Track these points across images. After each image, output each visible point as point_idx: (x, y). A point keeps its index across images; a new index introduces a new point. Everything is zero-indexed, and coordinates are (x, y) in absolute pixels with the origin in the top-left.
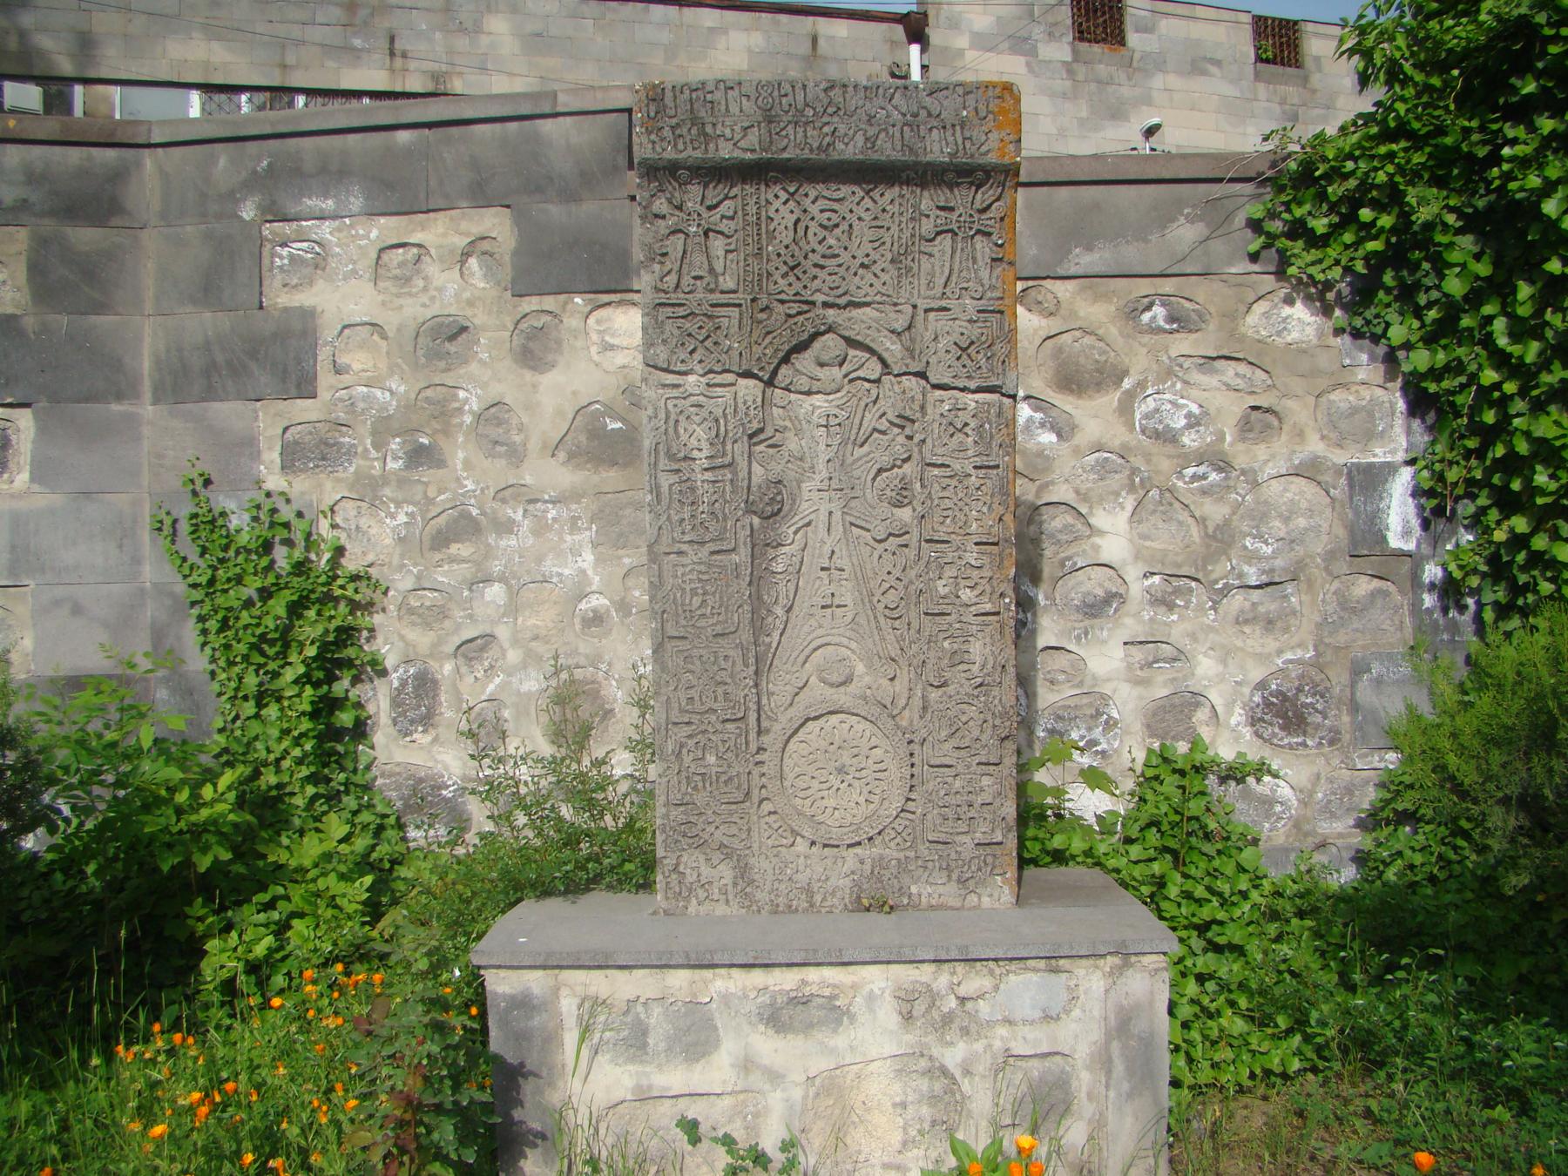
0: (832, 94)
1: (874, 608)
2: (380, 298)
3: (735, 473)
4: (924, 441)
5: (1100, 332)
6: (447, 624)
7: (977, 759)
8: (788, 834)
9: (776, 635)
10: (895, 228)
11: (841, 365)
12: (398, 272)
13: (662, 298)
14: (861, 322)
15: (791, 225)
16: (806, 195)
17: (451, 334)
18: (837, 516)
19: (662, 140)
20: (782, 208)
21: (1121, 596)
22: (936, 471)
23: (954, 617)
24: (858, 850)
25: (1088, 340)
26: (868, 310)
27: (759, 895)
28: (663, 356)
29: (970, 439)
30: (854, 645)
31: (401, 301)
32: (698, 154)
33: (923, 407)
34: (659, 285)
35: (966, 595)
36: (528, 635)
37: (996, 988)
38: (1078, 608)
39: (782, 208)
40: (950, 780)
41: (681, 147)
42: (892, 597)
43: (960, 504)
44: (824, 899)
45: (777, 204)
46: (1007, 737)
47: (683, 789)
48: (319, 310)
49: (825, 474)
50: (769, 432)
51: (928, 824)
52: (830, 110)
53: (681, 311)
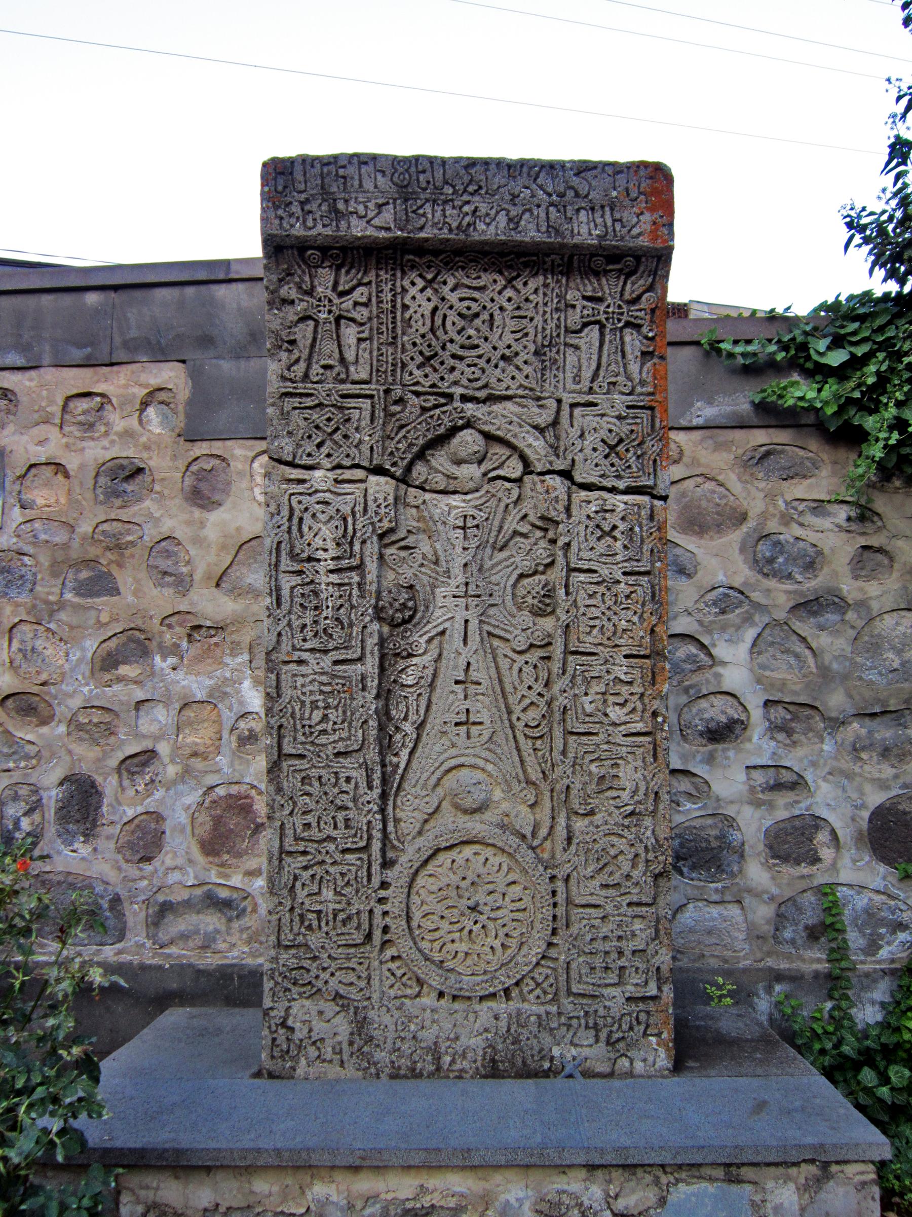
0: (473, 171)
1: (512, 727)
2: (64, 440)
3: (363, 576)
4: (568, 545)
5: (720, 478)
6: (112, 740)
7: (628, 899)
8: (413, 983)
9: (405, 754)
10: (538, 320)
11: (480, 462)
12: (81, 418)
13: (289, 387)
14: (499, 417)
15: (427, 313)
16: (445, 283)
17: (127, 475)
18: (474, 625)
19: (291, 215)
20: (418, 296)
21: (742, 722)
22: (582, 577)
23: (602, 736)
24: (492, 1004)
25: (710, 485)
26: (509, 405)
27: (379, 1055)
28: (289, 448)
29: (619, 544)
30: (490, 767)
31: (85, 444)
32: (328, 231)
33: (568, 509)
34: (286, 373)
35: (616, 713)
36: (188, 751)
37: (662, 1201)
38: (701, 734)
39: (418, 296)
40: (596, 922)
41: (310, 223)
42: (533, 715)
43: (608, 613)
44: (453, 1061)
45: (413, 291)
46: (660, 874)
47: (296, 929)
48: (8, 449)
49: (461, 579)
50: (402, 533)
51: (574, 974)
52: (471, 189)
53: (309, 402)
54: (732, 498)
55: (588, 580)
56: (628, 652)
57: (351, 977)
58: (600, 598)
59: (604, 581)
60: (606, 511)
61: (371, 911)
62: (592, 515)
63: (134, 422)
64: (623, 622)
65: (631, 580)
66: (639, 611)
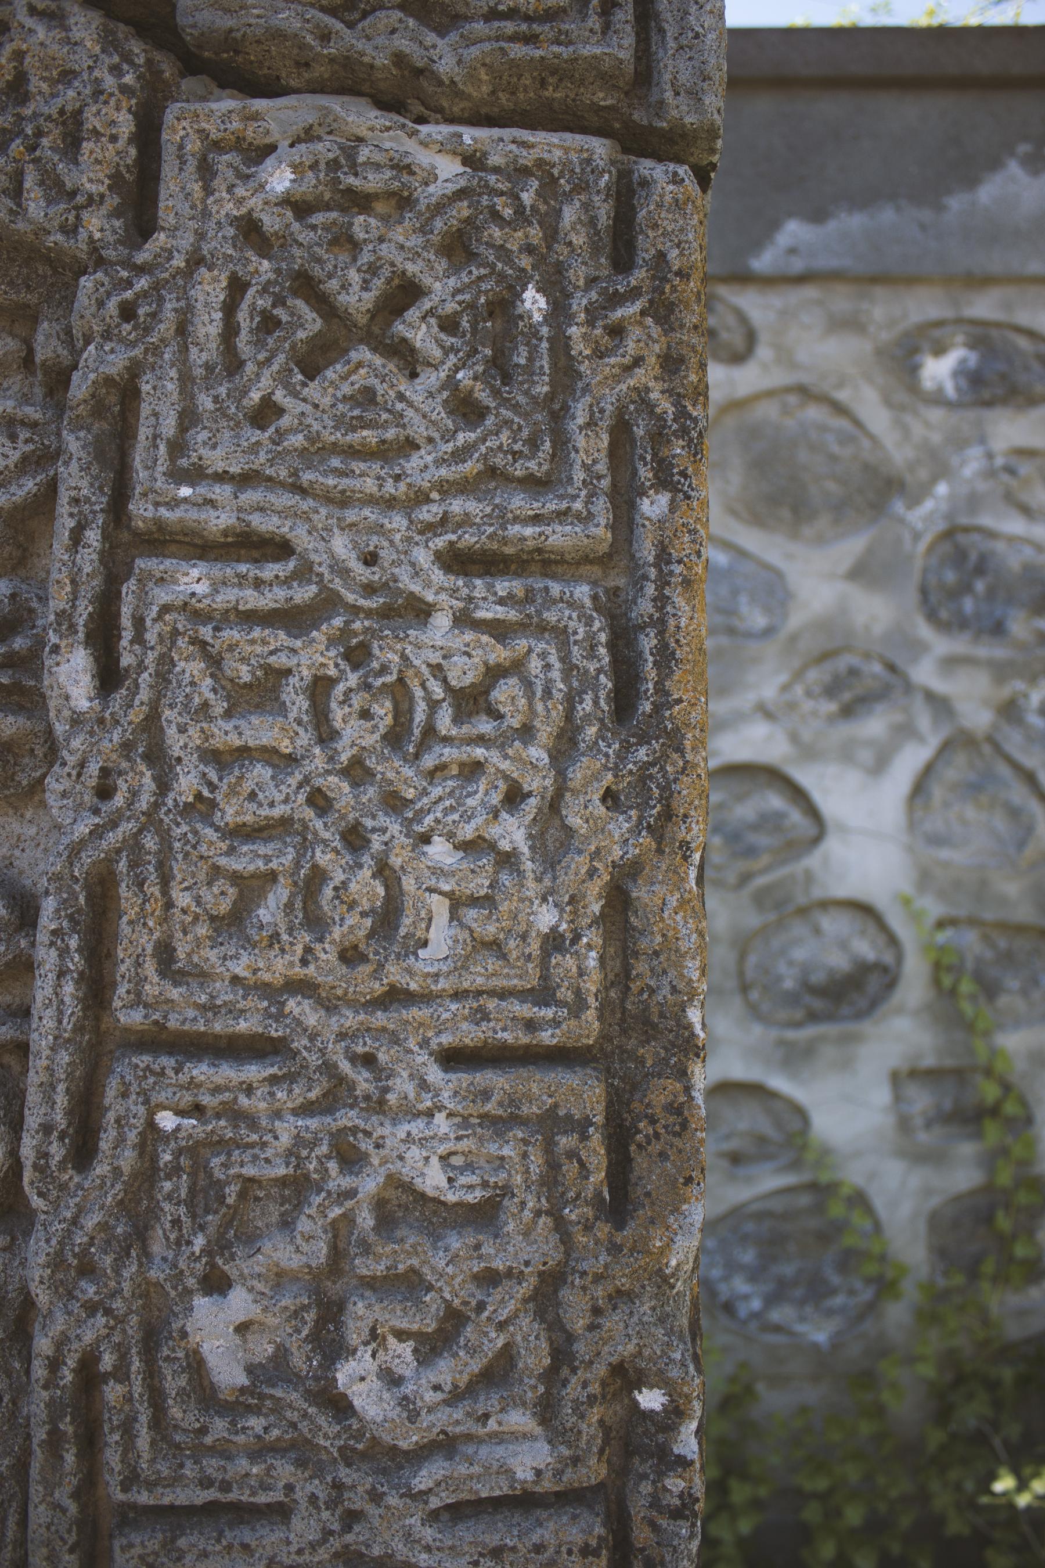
5: (843, 395)
21: (885, 969)
22: (194, 580)
25: (814, 413)
29: (430, 379)
54: (866, 443)
55: (228, 597)
56: (470, 1035)
58: (298, 704)
59: (329, 602)
60: (361, 202)
62: (270, 222)
64: (439, 851)
65: (492, 598)
66: (538, 785)
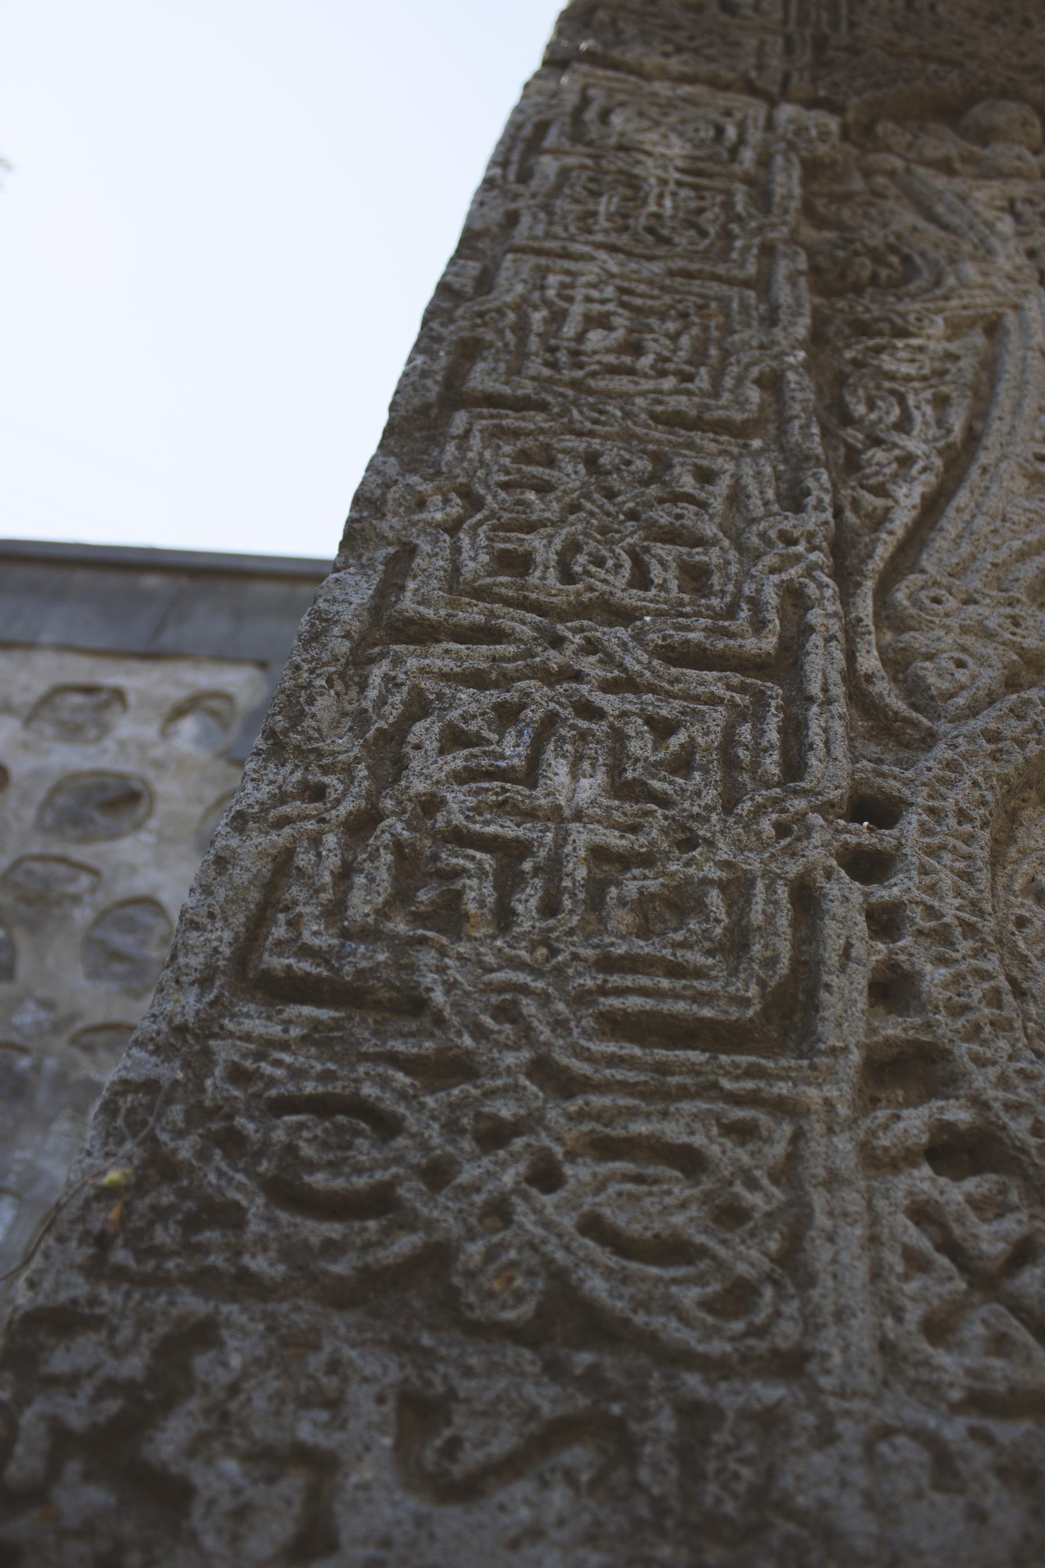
47: (361, 905)
57: (674, 1208)
61: (806, 899)
63: (151, 732)
